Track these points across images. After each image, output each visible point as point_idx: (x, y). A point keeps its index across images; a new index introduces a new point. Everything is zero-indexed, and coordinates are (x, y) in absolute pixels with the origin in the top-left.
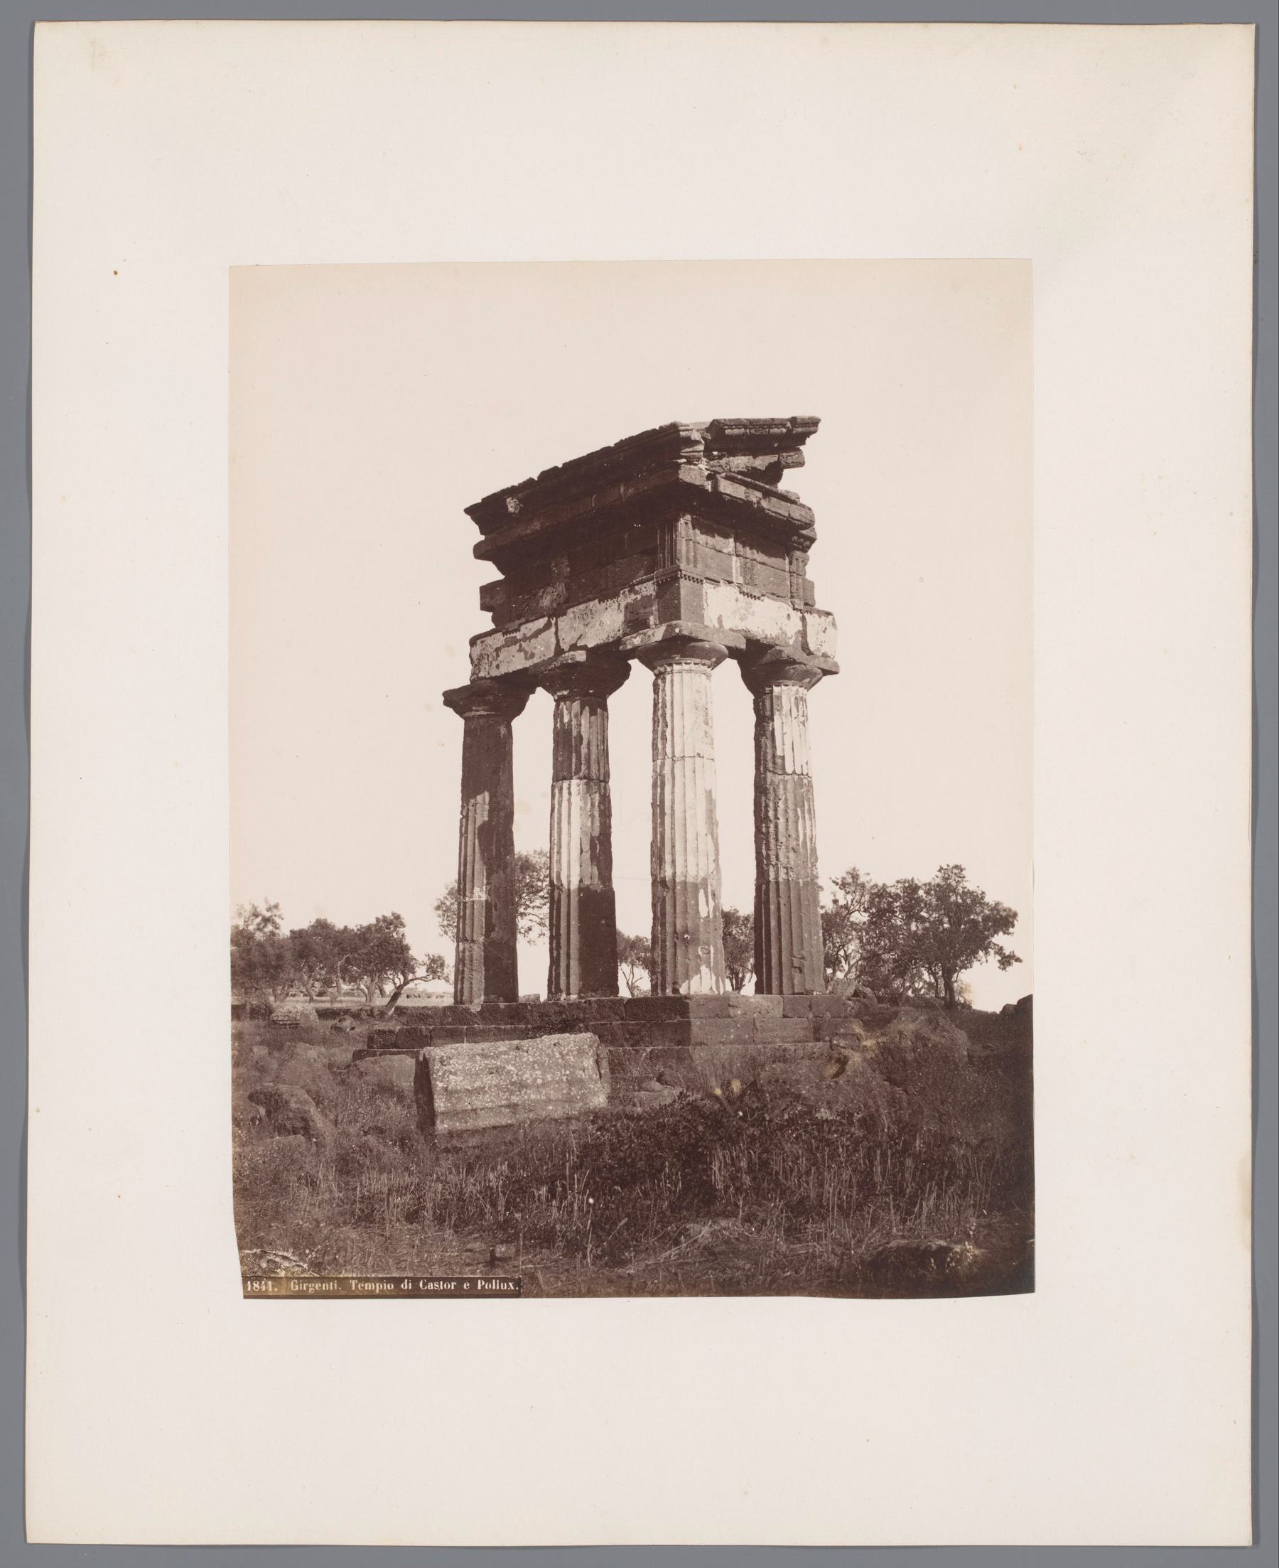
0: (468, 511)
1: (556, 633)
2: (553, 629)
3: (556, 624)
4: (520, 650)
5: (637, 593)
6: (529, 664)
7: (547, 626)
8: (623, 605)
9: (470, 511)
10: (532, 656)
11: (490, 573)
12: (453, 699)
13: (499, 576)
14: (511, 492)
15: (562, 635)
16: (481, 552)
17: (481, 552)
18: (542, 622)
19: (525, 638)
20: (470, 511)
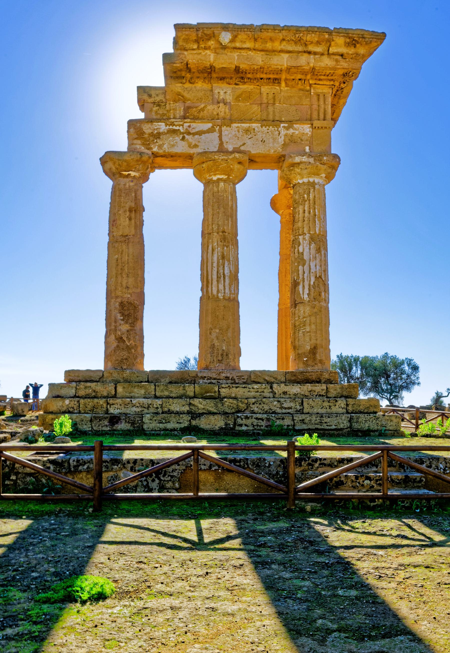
1: (220, 137)
2: (216, 134)
3: (220, 132)
5: (296, 129)
10: (196, 146)
14: (225, 27)
15: (224, 139)
19: (189, 133)
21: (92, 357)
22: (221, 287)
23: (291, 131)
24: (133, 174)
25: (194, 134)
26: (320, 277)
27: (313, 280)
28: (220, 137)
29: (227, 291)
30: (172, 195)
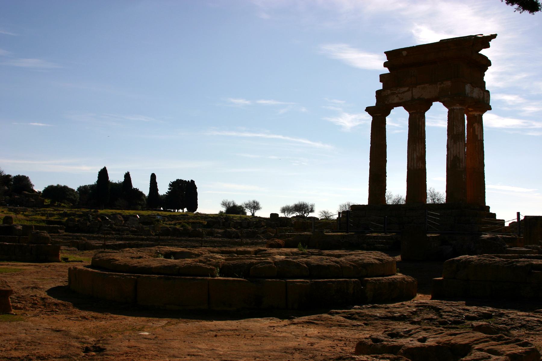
0: (385, 53)
1: (412, 93)
2: (411, 92)
3: (412, 90)
4: (397, 96)
6: (401, 101)
7: (408, 90)
8: (439, 87)
9: (387, 53)
10: (402, 99)
11: (386, 71)
12: (369, 110)
13: (389, 72)
15: (414, 94)
16: (386, 65)
17: (386, 65)
18: (406, 89)
19: (399, 93)
20: (387, 53)
21: (363, 199)
22: (412, 164)
23: (443, 85)
24: (378, 115)
25: (401, 93)
26: (456, 156)
27: (452, 157)
28: (412, 93)
29: (415, 166)
30: (398, 121)
